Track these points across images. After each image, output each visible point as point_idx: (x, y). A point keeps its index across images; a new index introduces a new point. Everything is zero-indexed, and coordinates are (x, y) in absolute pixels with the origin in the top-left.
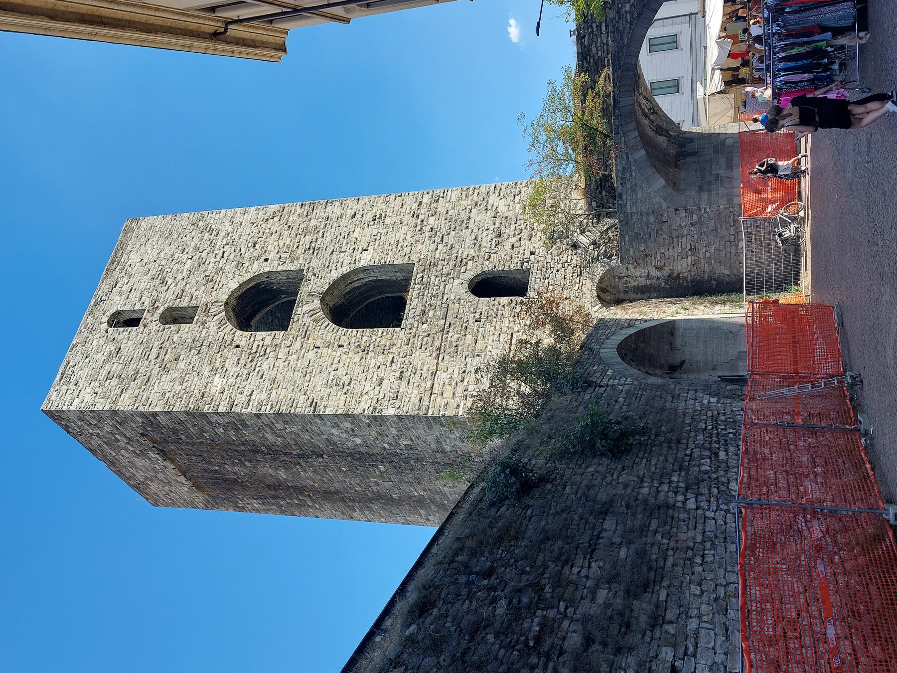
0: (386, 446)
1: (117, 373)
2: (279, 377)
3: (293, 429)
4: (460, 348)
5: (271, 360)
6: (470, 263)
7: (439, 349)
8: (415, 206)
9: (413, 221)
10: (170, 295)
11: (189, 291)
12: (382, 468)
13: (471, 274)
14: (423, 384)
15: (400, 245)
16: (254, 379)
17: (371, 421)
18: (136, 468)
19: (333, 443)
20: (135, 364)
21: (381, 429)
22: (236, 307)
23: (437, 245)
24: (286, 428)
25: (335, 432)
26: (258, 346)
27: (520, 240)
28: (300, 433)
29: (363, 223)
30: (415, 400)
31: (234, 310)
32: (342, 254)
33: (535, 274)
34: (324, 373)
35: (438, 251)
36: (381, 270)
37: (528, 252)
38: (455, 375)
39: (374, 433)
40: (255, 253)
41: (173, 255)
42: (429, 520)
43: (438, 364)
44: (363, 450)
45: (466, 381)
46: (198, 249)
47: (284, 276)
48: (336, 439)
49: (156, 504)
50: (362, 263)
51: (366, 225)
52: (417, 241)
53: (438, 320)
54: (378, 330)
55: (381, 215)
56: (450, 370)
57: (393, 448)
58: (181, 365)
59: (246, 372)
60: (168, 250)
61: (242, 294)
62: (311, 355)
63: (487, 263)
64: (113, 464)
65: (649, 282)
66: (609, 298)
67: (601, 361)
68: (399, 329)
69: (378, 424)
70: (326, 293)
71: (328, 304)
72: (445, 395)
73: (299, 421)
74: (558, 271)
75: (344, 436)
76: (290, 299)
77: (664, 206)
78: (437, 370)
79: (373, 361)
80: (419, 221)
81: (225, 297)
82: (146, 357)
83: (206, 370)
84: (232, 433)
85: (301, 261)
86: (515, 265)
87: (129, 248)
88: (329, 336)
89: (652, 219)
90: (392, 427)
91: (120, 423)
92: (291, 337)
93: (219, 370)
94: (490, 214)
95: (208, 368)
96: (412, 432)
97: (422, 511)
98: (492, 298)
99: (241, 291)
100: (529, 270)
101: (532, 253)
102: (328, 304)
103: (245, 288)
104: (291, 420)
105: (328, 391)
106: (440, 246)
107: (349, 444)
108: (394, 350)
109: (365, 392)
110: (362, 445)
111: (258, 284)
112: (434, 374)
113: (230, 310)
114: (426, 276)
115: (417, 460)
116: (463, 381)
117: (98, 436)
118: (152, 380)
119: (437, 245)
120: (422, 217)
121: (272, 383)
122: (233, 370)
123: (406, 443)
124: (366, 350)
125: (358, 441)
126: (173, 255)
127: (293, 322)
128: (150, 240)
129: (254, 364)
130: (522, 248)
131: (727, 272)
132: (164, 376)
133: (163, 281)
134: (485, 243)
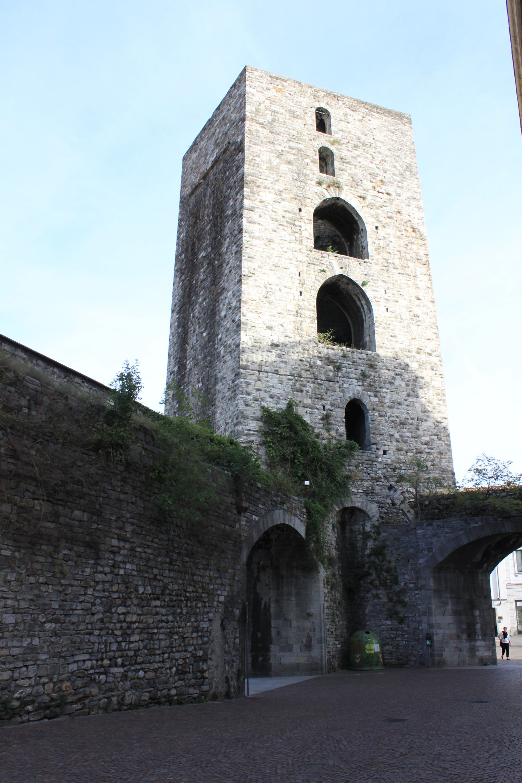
0: (219, 336)
1: (277, 119)
4: (299, 394)
5: (288, 238)
6: (376, 400)
7: (299, 376)
8: (428, 350)
9: (414, 349)
10: (345, 153)
11: (348, 168)
12: (205, 334)
13: (366, 400)
15: (392, 338)
16: (273, 225)
18: (208, 141)
19: (221, 293)
20: (284, 132)
23: (393, 371)
24: (232, 254)
25: (230, 293)
26: (300, 227)
27: (398, 441)
28: (229, 265)
29: (411, 306)
31: (334, 204)
35: (387, 371)
36: (370, 323)
37: (387, 448)
38: (275, 391)
39: (228, 325)
40: (382, 219)
41: (380, 153)
42: (171, 374)
43: (286, 375)
44: (217, 317)
45: (271, 400)
47: (364, 244)
48: (224, 295)
49: (184, 159)
51: (410, 309)
53: (326, 374)
55: (420, 321)
56: (280, 386)
58: (284, 167)
59: (278, 218)
60: (384, 150)
63: (377, 414)
64: (210, 124)
67: (268, 511)
71: (339, 280)
72: (258, 382)
74: (369, 474)
75: (227, 301)
76: (347, 249)
77: (421, 561)
78: (280, 375)
80: (414, 353)
81: (343, 197)
82: (291, 139)
83: (280, 186)
84: (229, 212)
85: (377, 256)
87: (385, 118)
88: (309, 284)
89: (412, 550)
91: (237, 125)
93: (279, 197)
94: (421, 415)
95: (281, 189)
97: (176, 369)
98: (344, 420)
100: (370, 450)
101: (385, 452)
102: (339, 280)
106: (392, 373)
107: (221, 306)
109: (261, 315)
110: (220, 317)
112: (276, 372)
114: (364, 362)
115: (211, 362)
116: (271, 397)
117: (229, 110)
118: (271, 146)
119: (393, 371)
120: (418, 356)
122: (280, 208)
123: (222, 352)
125: (223, 313)
126: (380, 153)
128: (392, 134)
129: (285, 224)
130: (389, 443)
131: (367, 611)
132: (275, 155)
133: (356, 147)
134: (395, 412)
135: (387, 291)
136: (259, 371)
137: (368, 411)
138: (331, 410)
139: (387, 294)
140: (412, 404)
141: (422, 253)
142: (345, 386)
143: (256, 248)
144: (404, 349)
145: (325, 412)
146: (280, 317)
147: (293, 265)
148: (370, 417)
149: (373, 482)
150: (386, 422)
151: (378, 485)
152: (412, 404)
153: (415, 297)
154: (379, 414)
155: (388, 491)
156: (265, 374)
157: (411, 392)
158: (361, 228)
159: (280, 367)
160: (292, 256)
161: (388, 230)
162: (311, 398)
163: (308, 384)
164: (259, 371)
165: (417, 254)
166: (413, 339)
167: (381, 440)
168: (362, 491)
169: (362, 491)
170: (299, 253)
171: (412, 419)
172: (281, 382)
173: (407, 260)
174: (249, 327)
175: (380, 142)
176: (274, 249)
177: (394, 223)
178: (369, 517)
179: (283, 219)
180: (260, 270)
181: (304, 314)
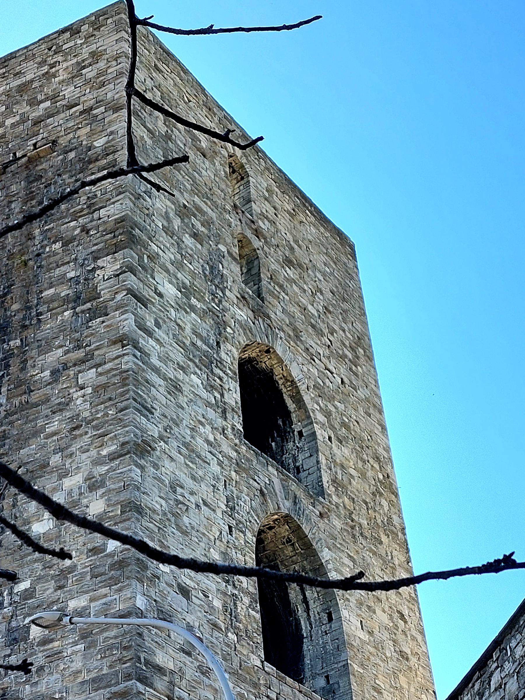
0: (23, 586)
2: (183, 400)
3: (79, 402)
5: (204, 394)
17: (111, 555)
21: (83, 575)
22: (253, 366)
34: (189, 483)
46: (332, 334)
47: (310, 463)
57: (17, 599)
61: (274, 383)
62: (215, 468)
69: (101, 570)
73: (107, 415)
90: (92, 600)
96: (75, 643)
99: (280, 382)
102: (271, 528)
103: (284, 390)
104: (110, 399)
111: (286, 414)
113: (254, 355)
121: (173, 383)
127: (257, 454)
132: (173, 207)
158: (297, 427)
160: (211, 438)
161: (346, 451)
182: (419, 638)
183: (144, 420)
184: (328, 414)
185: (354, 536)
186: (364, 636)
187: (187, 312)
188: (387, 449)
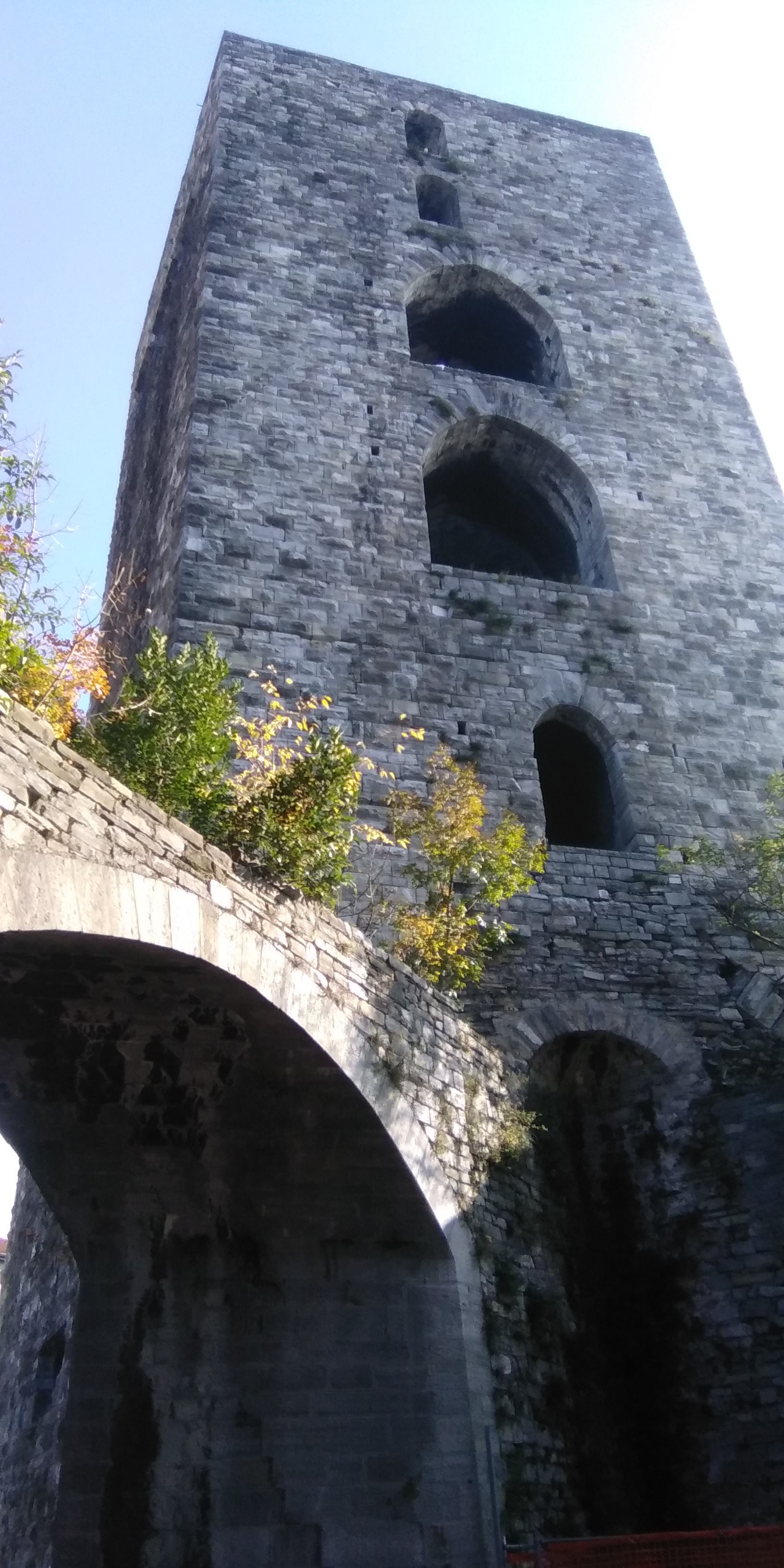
4: (377, 688)
5: (338, 333)
6: (634, 709)
7: (374, 641)
14: (270, 608)
15: (666, 561)
16: (288, 307)
30: (225, 591)
31: (467, 297)
32: (623, 454)
33: (622, 862)
34: (303, 420)
40: (601, 312)
50: (602, 490)
52: (682, 595)
53: (459, 640)
54: (422, 518)
56: (312, 666)
58: (320, 202)
62: (349, 397)
63: (642, 747)
65: (643, 1198)
66: (580, 1080)
68: (428, 558)
70: (518, 430)
78: (311, 638)
79: (337, 509)
81: (486, 263)
86: (636, 813)
92: (396, 365)
93: (307, 255)
98: (535, 761)
99: (508, 299)
105: (255, 427)
108: (368, 550)
109: (250, 493)
112: (299, 629)
119: (677, 637)
120: (752, 605)
122: (310, 277)
124: (365, 495)
133: (515, 181)
134: (700, 742)
135: (632, 455)
136: (241, 626)
137: (610, 740)
138: (487, 734)
139: (635, 462)
140: (757, 723)
141: (722, 381)
142: (526, 670)
143: (239, 348)
144: (705, 585)
145: (466, 739)
146: (309, 499)
147: (351, 390)
148: (619, 756)
149: (663, 951)
150: (678, 769)
151: (682, 959)
152: (757, 723)
153: (719, 470)
154: (651, 748)
155: (723, 981)
156: (263, 635)
157: (745, 691)
159: (311, 618)
162: (416, 699)
163: (403, 664)
164: (241, 626)
165: (708, 383)
166: (728, 563)
167: (670, 820)
168: (623, 978)
169: (623, 978)
170: (368, 366)
171: (765, 762)
172: (311, 656)
173: (682, 393)
174: (212, 516)
175: (577, 176)
176: (293, 354)
177: (634, 320)
178: (663, 1069)
179: (320, 298)
180: (252, 394)
181: (387, 494)
182: (766, 488)
183: (218, 378)
184: (584, 307)
185: (629, 413)
186: (647, 505)
187: (310, 266)
188: (709, 316)
